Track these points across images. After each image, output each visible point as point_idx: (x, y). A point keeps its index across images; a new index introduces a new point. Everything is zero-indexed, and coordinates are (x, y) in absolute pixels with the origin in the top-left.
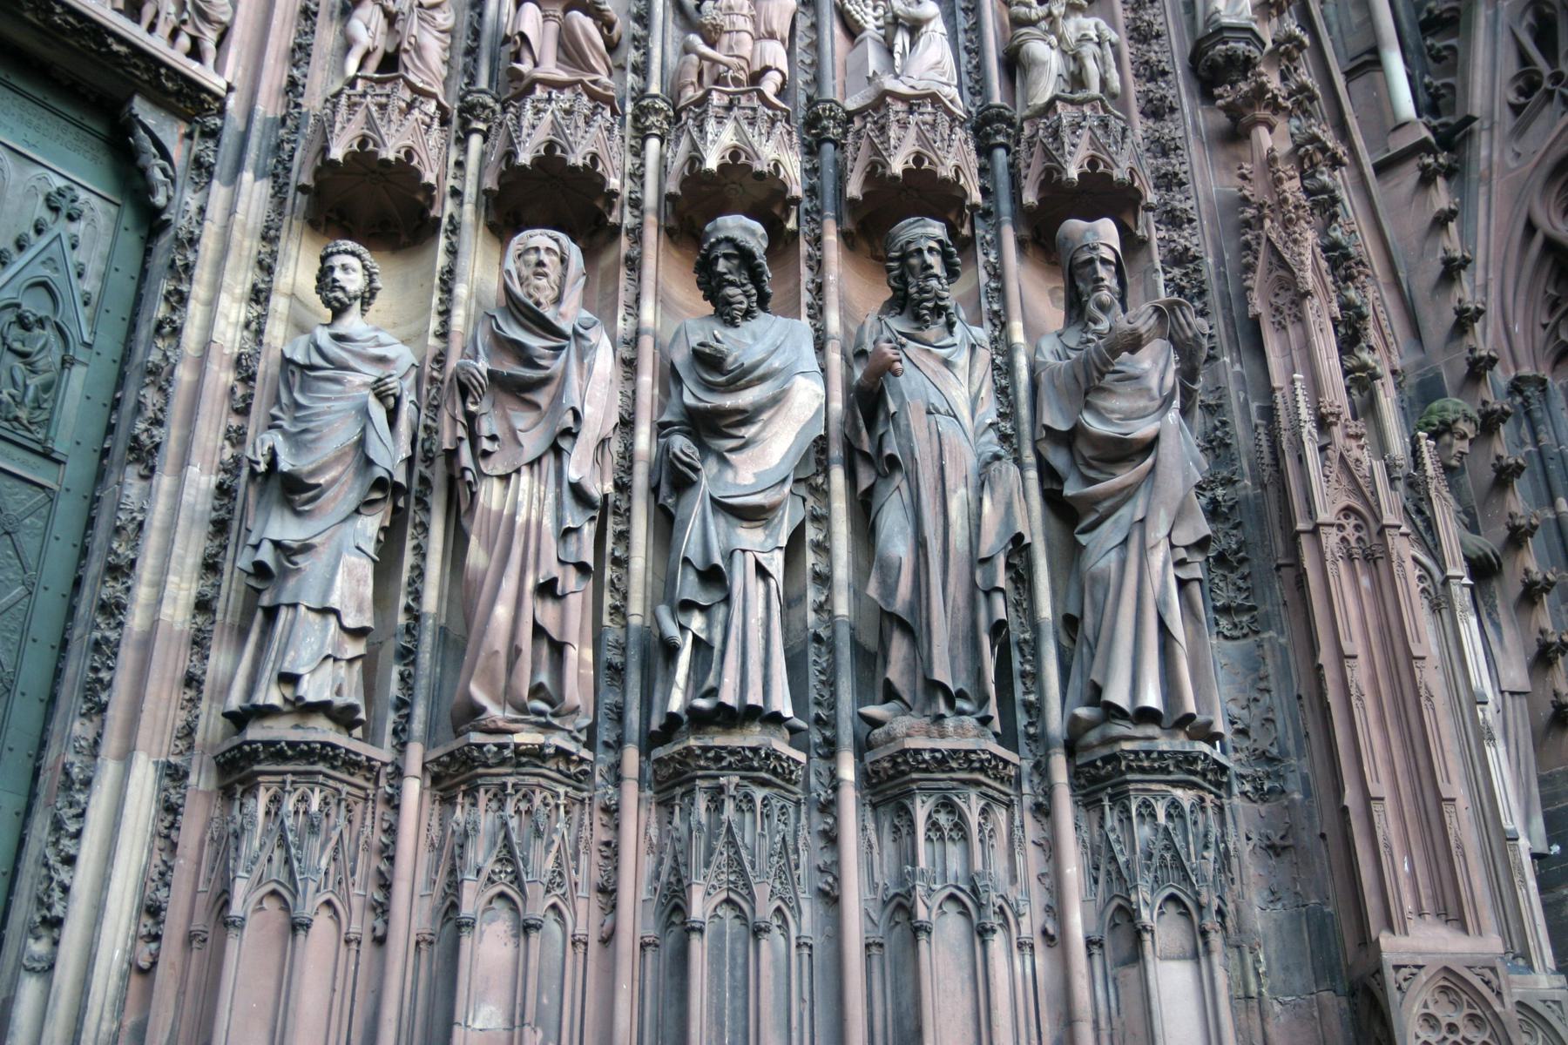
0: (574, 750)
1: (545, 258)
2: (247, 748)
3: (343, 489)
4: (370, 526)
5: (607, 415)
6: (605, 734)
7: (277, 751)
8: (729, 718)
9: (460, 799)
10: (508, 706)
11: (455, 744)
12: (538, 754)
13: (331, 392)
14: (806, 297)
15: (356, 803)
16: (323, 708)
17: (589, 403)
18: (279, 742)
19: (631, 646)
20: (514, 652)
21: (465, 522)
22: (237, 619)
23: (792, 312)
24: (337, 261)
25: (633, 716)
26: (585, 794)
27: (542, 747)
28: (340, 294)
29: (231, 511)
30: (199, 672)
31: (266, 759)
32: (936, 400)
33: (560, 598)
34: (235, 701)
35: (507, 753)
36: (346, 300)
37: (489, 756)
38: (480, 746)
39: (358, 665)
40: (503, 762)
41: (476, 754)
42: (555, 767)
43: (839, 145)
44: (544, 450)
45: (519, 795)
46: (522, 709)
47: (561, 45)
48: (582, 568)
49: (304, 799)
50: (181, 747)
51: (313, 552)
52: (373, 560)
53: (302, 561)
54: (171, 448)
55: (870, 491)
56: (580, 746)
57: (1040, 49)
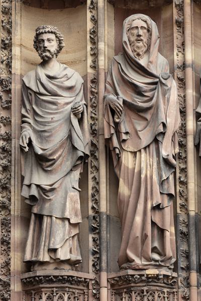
0: (170, 275)
1: (141, 32)
2: (37, 278)
3: (64, 162)
4: (76, 174)
6: (183, 264)
7: (49, 279)
9: (124, 296)
10: (143, 258)
11: (122, 273)
12: (156, 278)
13: (52, 109)
15: (80, 296)
16: (68, 262)
17: (169, 117)
18: (50, 276)
19: (191, 226)
20: (144, 237)
21: (117, 171)
22: (19, 213)
26: (174, 290)
27: (158, 275)
28: (48, 54)
29: (10, 162)
30: (8, 239)
31: (45, 282)
35: (143, 278)
36: (51, 56)
37: (136, 280)
38: (133, 276)
39: (76, 238)
40: (142, 281)
41: (131, 279)
42: (163, 282)
44: (152, 141)
45: (149, 294)
48: (170, 196)
50: (4, 272)
51: (55, 191)
52: (79, 191)
53: (52, 196)
56: (171, 271)
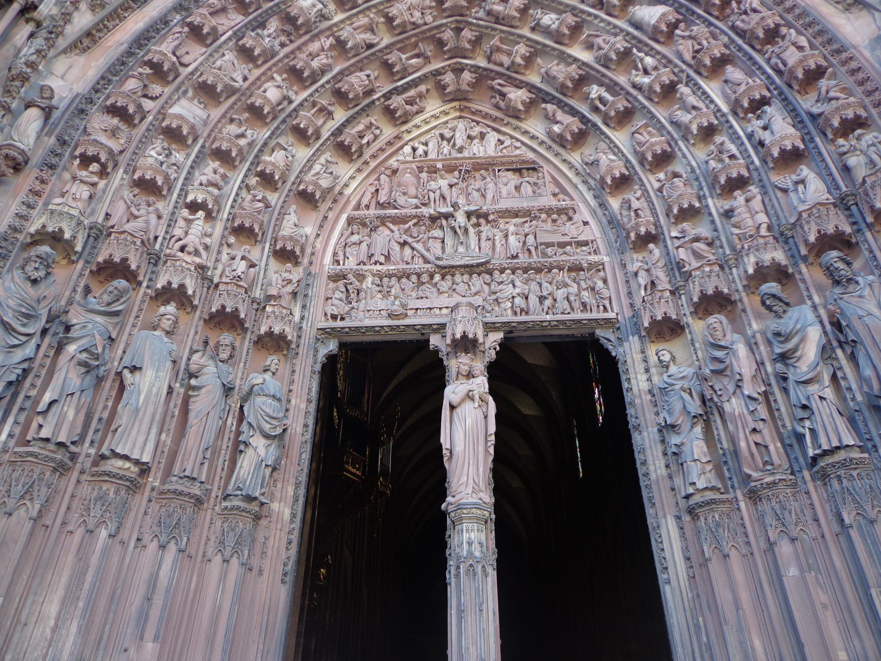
1: (715, 325)
4: (698, 429)
5: (750, 368)
7: (700, 505)
8: (825, 453)
11: (748, 488)
12: (774, 483)
14: (805, 293)
20: (752, 455)
23: (802, 302)
24: (660, 354)
25: (801, 460)
32: (861, 313)
33: (760, 432)
34: (683, 494)
39: (713, 471)
40: (765, 488)
43: (793, 237)
46: (763, 471)
47: (694, 254)
49: (713, 517)
54: (643, 423)
55: (852, 353)
57: (852, 161)
